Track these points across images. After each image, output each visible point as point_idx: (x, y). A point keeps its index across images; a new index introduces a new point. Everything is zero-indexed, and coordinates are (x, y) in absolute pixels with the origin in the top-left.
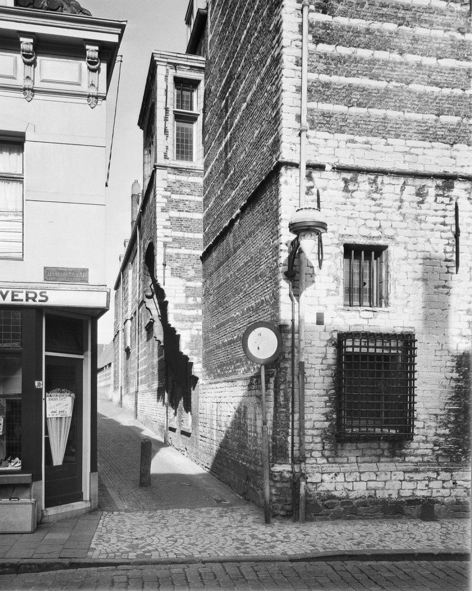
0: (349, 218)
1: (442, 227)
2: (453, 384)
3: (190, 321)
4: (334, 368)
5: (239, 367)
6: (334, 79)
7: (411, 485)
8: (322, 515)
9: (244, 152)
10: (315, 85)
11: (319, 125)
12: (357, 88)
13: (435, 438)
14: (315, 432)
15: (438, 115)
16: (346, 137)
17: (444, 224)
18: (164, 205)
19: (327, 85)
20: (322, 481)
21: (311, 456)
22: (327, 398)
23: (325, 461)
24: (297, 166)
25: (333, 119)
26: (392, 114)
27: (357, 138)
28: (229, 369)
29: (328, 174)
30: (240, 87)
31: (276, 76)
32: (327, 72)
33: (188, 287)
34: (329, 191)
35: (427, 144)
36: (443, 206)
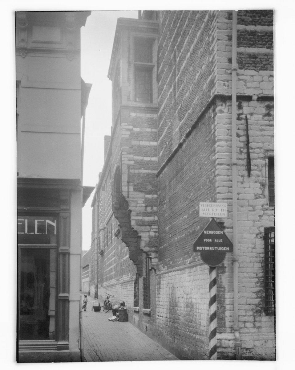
3: (148, 225)
4: (263, 255)
5: (186, 258)
9: (189, 91)
10: (243, 34)
11: (247, 65)
18: (128, 136)
19: (253, 33)
21: (245, 327)
22: (257, 280)
24: (230, 98)
25: (258, 60)
28: (179, 261)
29: (253, 103)
30: (185, 40)
31: (213, 29)
33: (147, 199)
34: (255, 116)
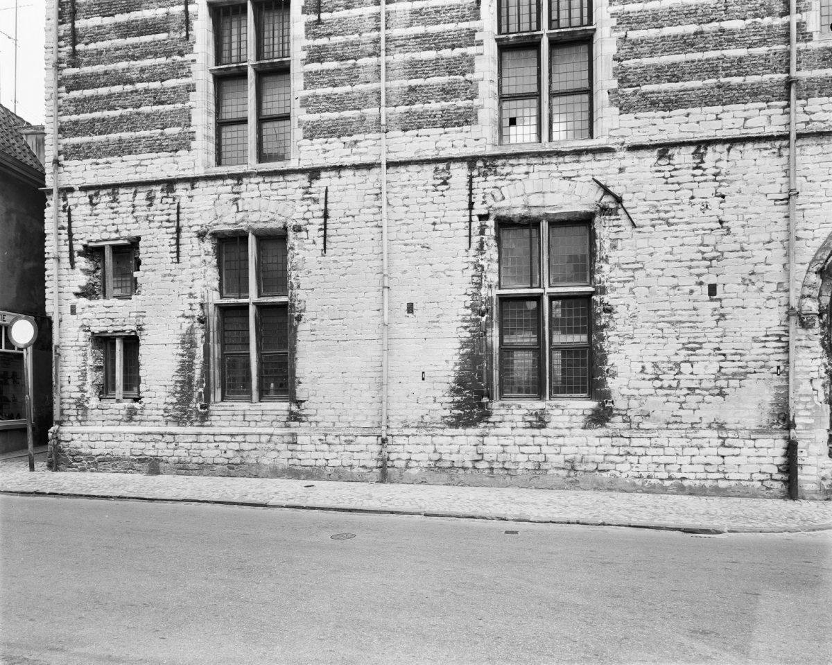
0: (94, 226)
1: (168, 224)
2: (180, 358)
6: (83, 117)
7: (142, 445)
12: (98, 120)
13: (165, 405)
14: (71, 401)
15: (162, 129)
16: (91, 160)
17: (168, 221)
19: (76, 123)
23: (79, 424)
25: (81, 149)
26: (126, 135)
27: (99, 161)
32: (76, 112)
34: (79, 207)
35: (154, 155)
36: (167, 206)
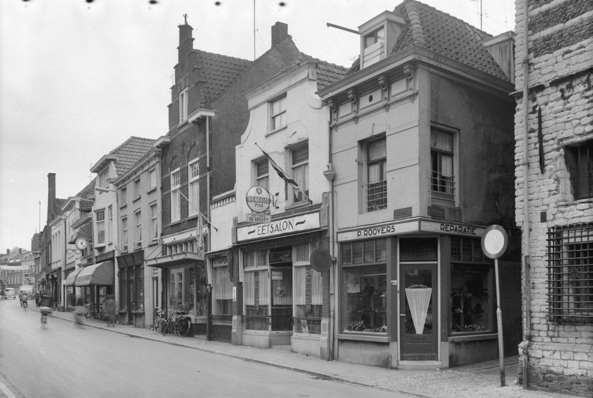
8: (543, 386)
20: (543, 357)
21: (539, 336)
23: (549, 340)
25: (552, 40)
29: (549, 90)
34: (550, 104)
